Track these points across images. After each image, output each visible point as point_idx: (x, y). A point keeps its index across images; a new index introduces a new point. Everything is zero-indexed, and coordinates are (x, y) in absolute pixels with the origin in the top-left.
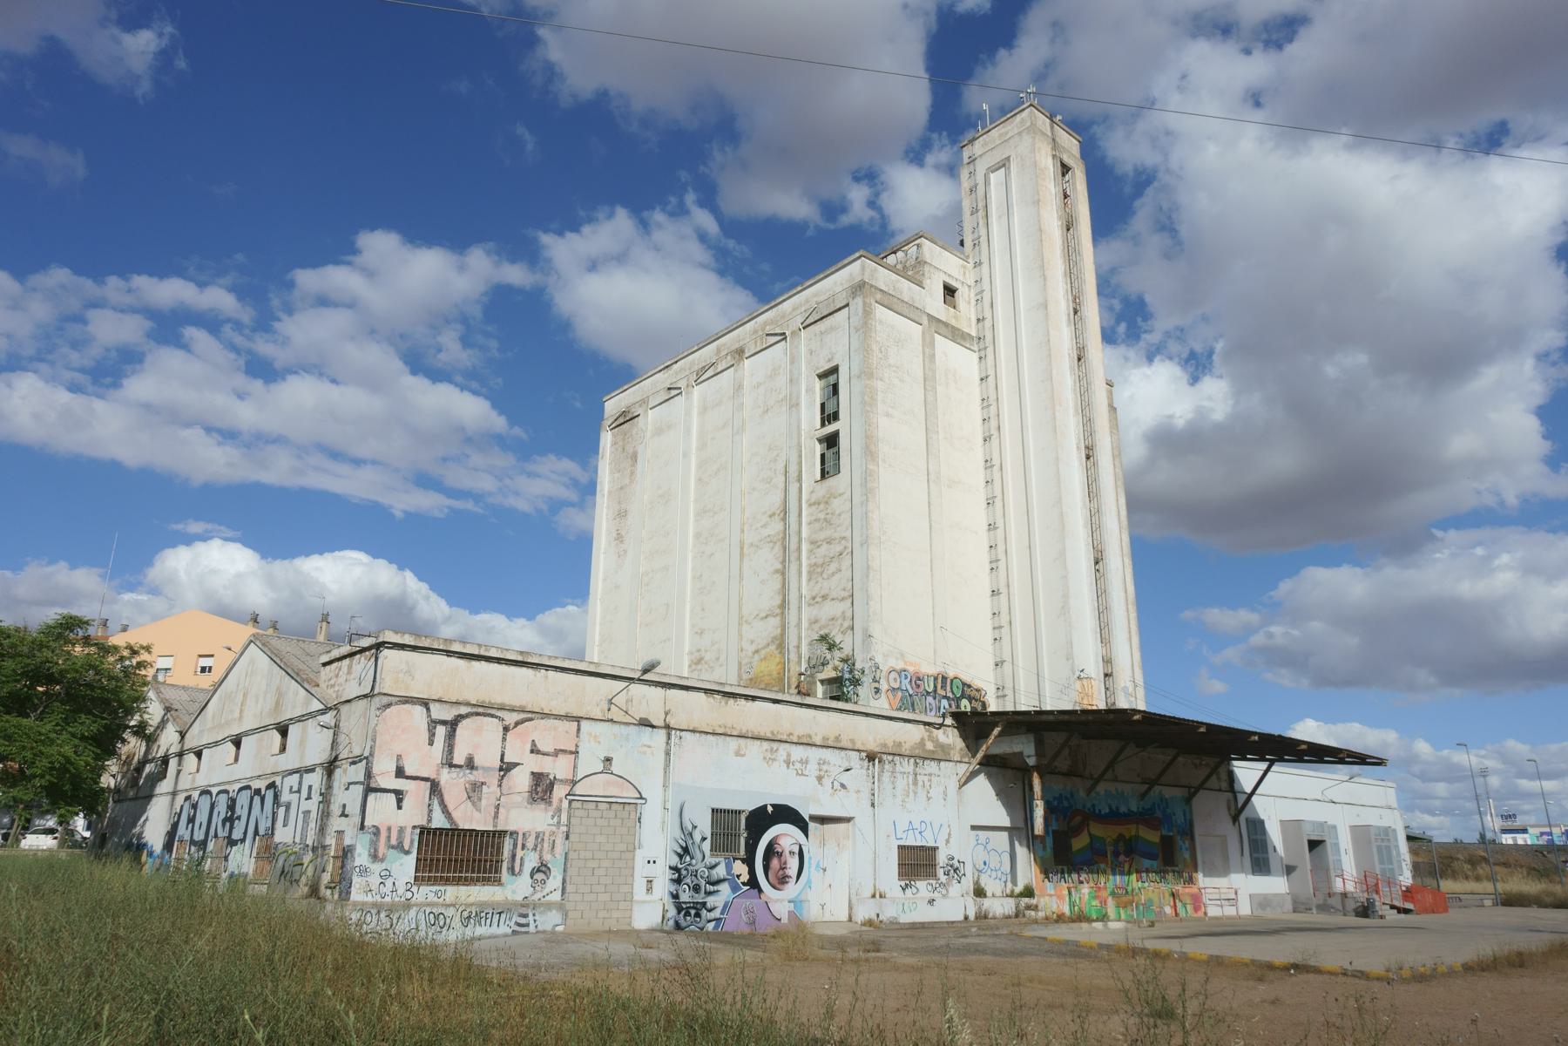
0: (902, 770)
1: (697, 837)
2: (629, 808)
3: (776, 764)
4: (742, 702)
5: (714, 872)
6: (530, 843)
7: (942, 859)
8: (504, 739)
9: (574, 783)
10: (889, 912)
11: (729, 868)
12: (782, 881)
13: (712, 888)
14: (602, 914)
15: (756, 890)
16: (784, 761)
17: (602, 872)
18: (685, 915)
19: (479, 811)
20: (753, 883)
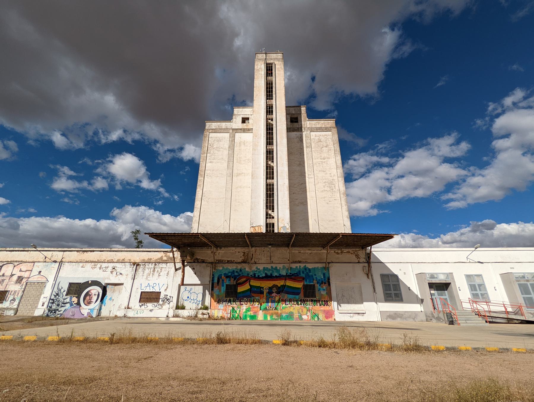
0: (148, 267)
1: (62, 291)
2: (42, 285)
3: (96, 269)
4: (90, 252)
5: (65, 300)
6: (13, 293)
7: (162, 296)
8: (13, 269)
9: (29, 278)
10: (131, 314)
11: (71, 299)
12: (89, 303)
13: (63, 305)
14: (28, 311)
15: (79, 306)
16: (99, 268)
17: (31, 300)
18: (51, 312)
19: (2, 286)
20: (78, 304)
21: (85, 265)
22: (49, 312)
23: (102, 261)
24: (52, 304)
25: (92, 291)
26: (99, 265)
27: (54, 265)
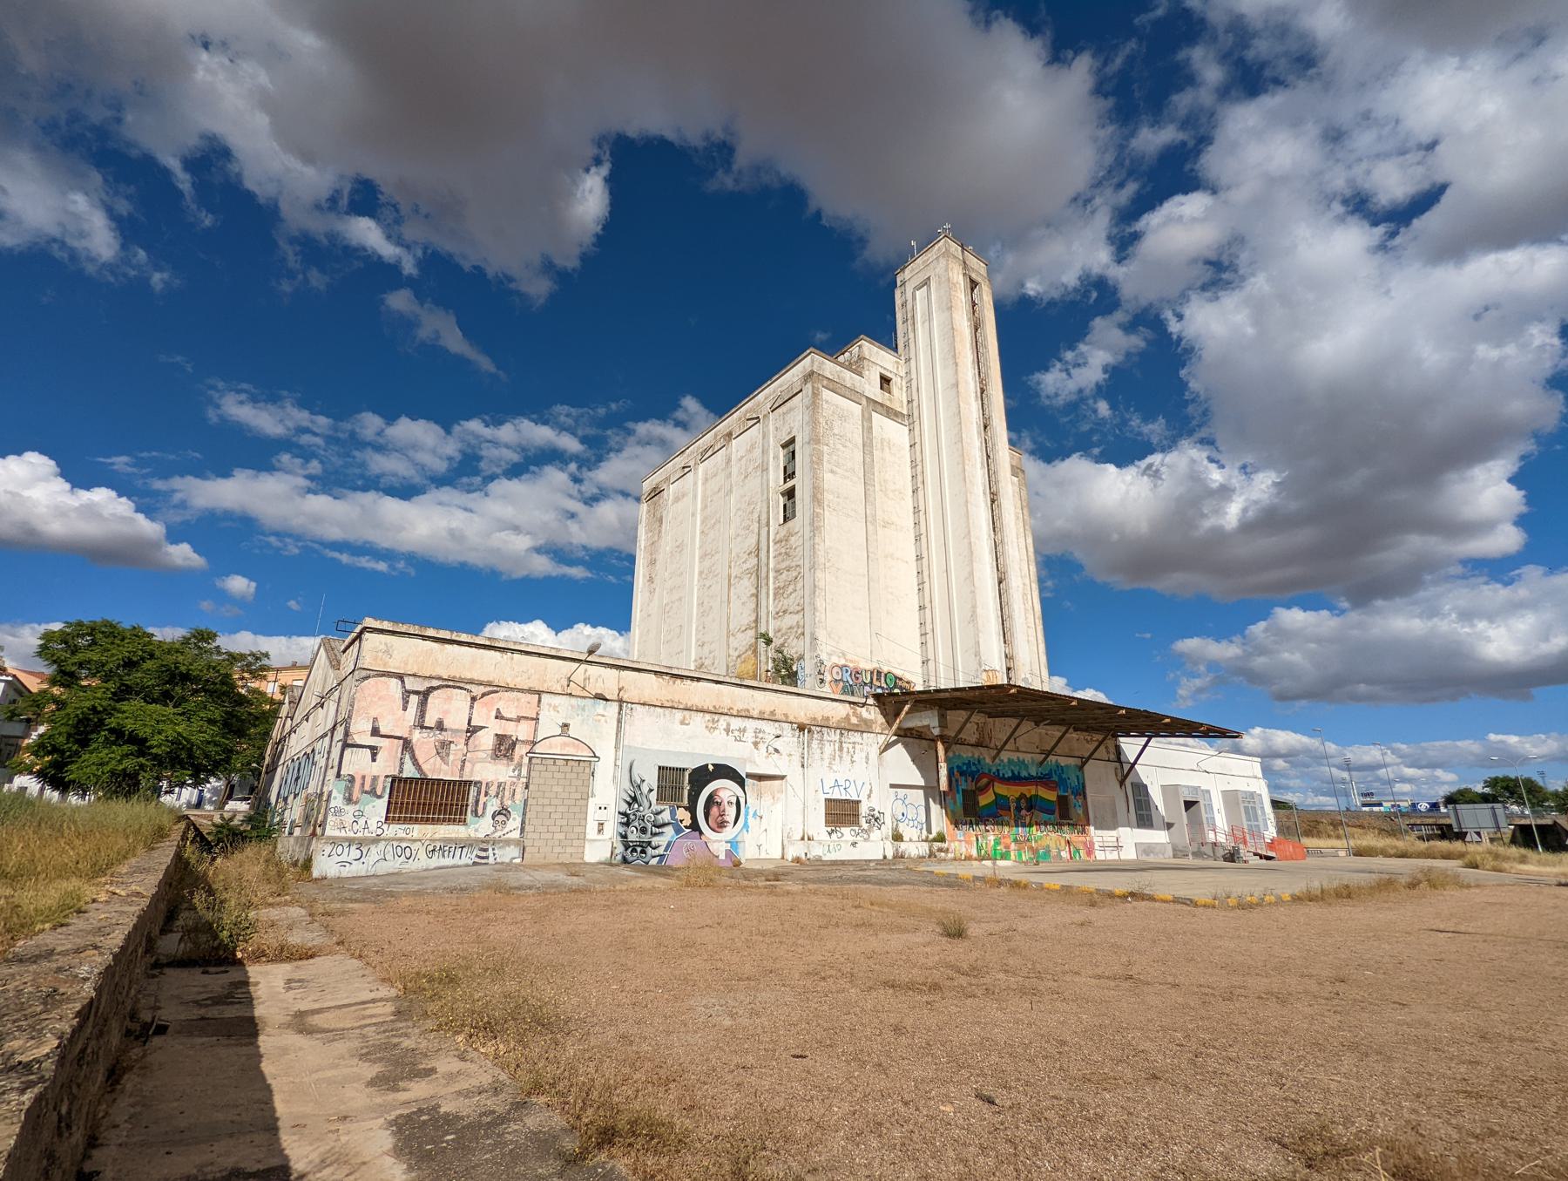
1: (645, 789)
2: (584, 766)
3: (717, 732)
4: (689, 682)
5: (659, 817)
6: (492, 791)
7: (864, 809)
8: (472, 707)
9: (534, 743)
10: (816, 851)
11: (673, 814)
12: (721, 825)
13: (655, 830)
14: (557, 850)
15: (697, 833)
17: (558, 816)
18: (632, 852)
19: (448, 764)
20: (695, 826)
21: (688, 717)
22: (626, 850)
23: (726, 711)
24: (625, 828)
25: (721, 794)
26: (723, 721)
27: (605, 709)
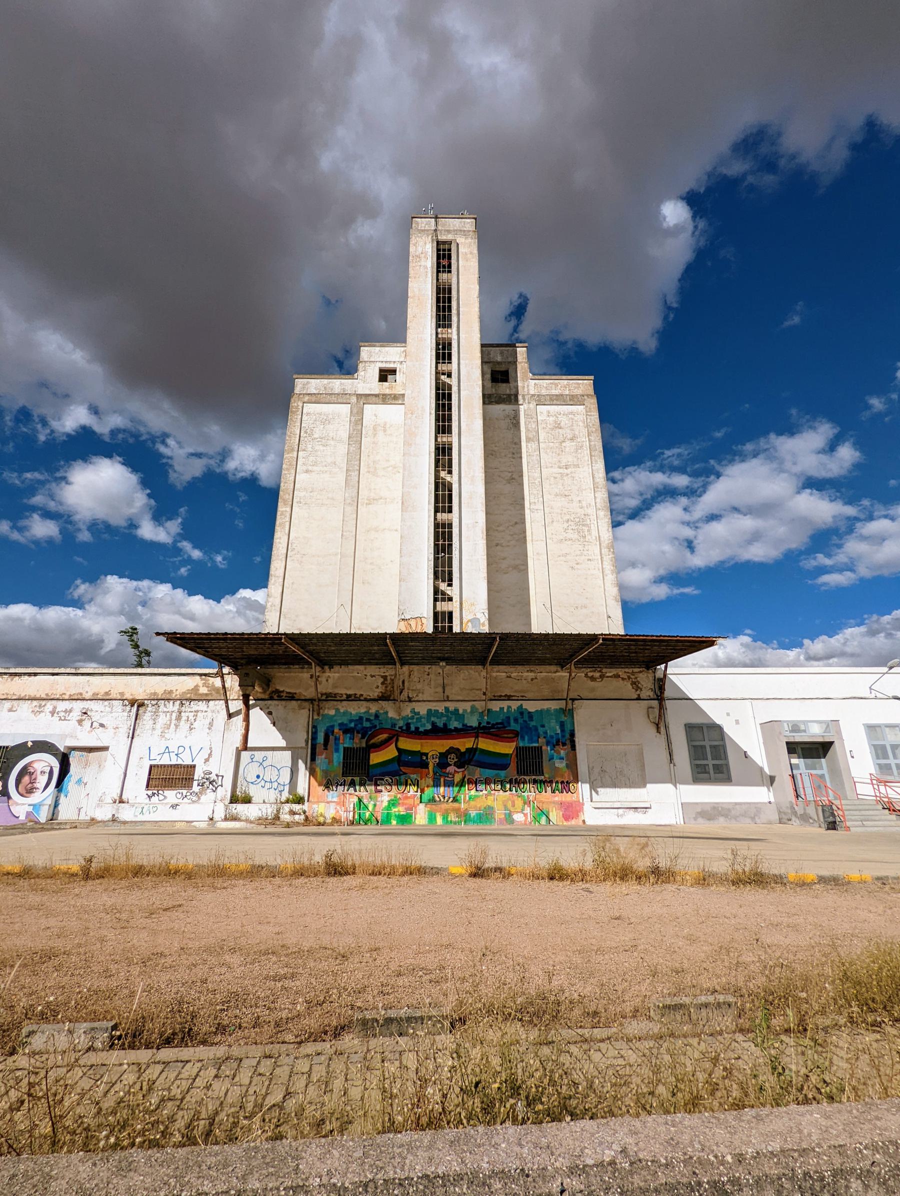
0: (165, 710)
3: (42, 714)
4: (26, 677)
7: (198, 774)
10: (126, 814)
12: (30, 791)
16: (50, 712)
23: (58, 696)
25: (35, 765)
26: (49, 706)
